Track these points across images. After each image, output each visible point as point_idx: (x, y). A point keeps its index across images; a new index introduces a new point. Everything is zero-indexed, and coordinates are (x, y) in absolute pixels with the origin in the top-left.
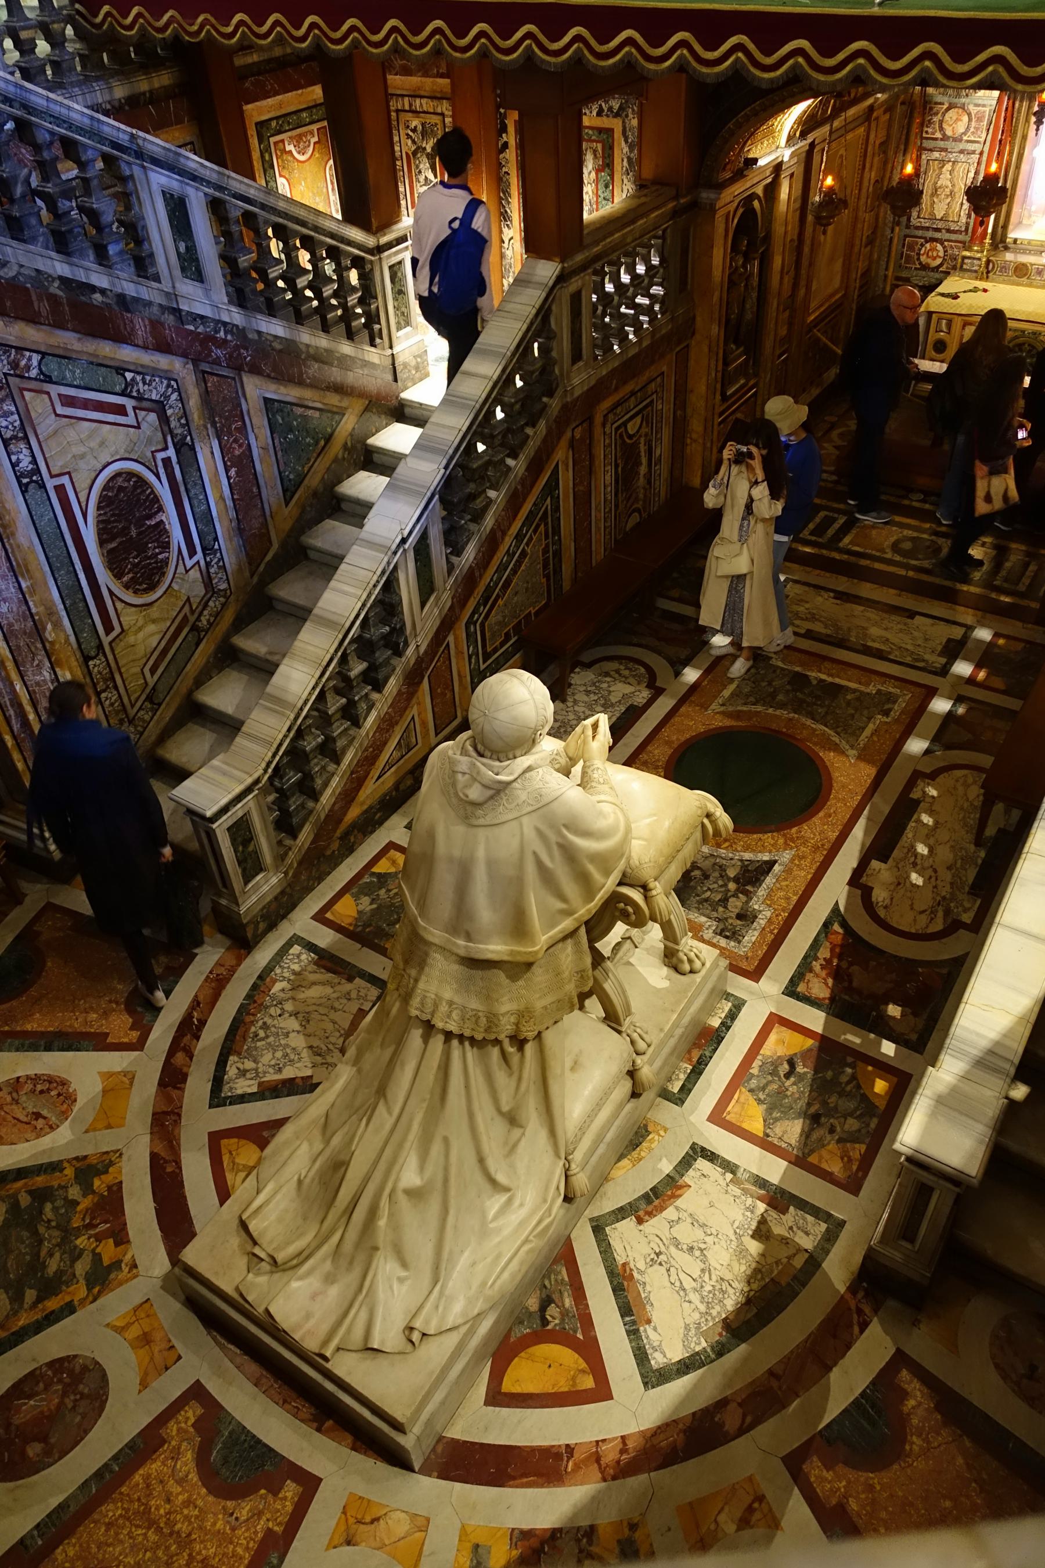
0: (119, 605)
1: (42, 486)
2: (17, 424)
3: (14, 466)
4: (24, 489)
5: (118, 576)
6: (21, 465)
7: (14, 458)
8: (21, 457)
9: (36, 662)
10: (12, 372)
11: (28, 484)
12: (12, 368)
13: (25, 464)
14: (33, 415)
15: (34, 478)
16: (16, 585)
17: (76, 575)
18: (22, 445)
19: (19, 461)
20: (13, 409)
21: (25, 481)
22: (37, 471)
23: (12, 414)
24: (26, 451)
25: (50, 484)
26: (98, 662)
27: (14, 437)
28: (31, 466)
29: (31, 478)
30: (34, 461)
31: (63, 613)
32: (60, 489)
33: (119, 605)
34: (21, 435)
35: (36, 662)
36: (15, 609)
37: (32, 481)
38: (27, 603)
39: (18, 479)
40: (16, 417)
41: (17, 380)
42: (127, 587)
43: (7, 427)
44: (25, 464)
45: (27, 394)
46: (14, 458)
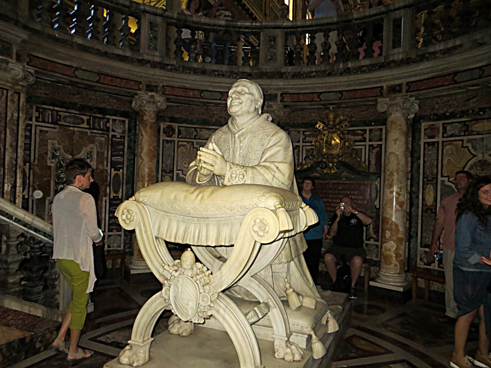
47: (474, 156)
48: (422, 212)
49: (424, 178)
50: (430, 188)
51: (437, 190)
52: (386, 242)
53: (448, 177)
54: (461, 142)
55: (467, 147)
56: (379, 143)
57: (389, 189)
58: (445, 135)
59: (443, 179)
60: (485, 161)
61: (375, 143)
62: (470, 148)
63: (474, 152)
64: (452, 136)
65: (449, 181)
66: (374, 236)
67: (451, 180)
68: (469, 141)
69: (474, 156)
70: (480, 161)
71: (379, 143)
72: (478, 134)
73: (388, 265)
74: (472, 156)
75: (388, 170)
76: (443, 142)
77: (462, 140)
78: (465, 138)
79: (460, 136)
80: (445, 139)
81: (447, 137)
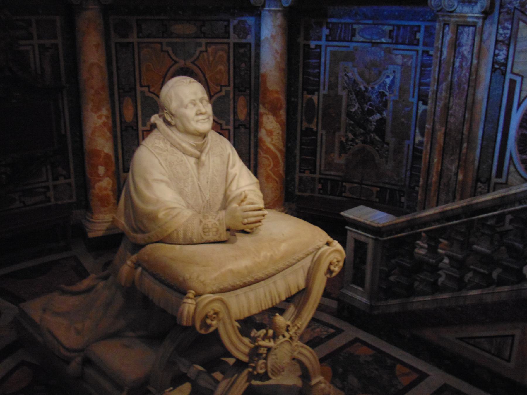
0: (512, 168)
1: (504, 74)
2: (508, 35)
3: (495, 55)
4: (493, 70)
5: (521, 151)
6: (499, 57)
7: (497, 52)
8: (501, 53)
9: (452, 158)
10: (519, 8)
11: (496, 69)
12: (520, 6)
13: (501, 58)
14: (519, 35)
15: (502, 68)
16: (463, 113)
17: (497, 133)
18: (504, 48)
19: (498, 55)
20: (510, 27)
21: (496, 66)
22: (505, 65)
23: (508, 29)
24: (505, 52)
25: (509, 76)
26: (483, 187)
27: (503, 42)
28: (503, 61)
29: (501, 66)
30: (506, 59)
31: (479, 147)
32: (513, 82)
33: (512, 168)
34: (506, 42)
35: (452, 158)
36: (457, 124)
37: (499, 69)
38: (463, 126)
39: (494, 63)
40: (509, 32)
41: (520, 13)
42: (523, 162)
43: (501, 34)
44: (501, 58)
45: (521, 24)
46: (497, 52)
47: (176, 62)
48: (122, 131)
49: (119, 89)
50: (128, 101)
51: (136, 103)
52: (100, 181)
53: (148, 86)
54: (159, 46)
55: (167, 52)
56: (53, 41)
57: (96, 113)
58: (140, 35)
59: (143, 89)
60: (187, 68)
61: (47, 42)
62: (171, 52)
63: (174, 58)
64: (148, 36)
65: (149, 92)
66: (64, 173)
67: (151, 90)
68: (169, 44)
69: (176, 62)
70: (182, 69)
71: (53, 41)
72: (178, 36)
73: (106, 206)
74: (173, 62)
75: (92, 88)
76: (139, 43)
77: (161, 43)
78: (165, 41)
79: (158, 37)
80: (140, 40)
81: (144, 37)
